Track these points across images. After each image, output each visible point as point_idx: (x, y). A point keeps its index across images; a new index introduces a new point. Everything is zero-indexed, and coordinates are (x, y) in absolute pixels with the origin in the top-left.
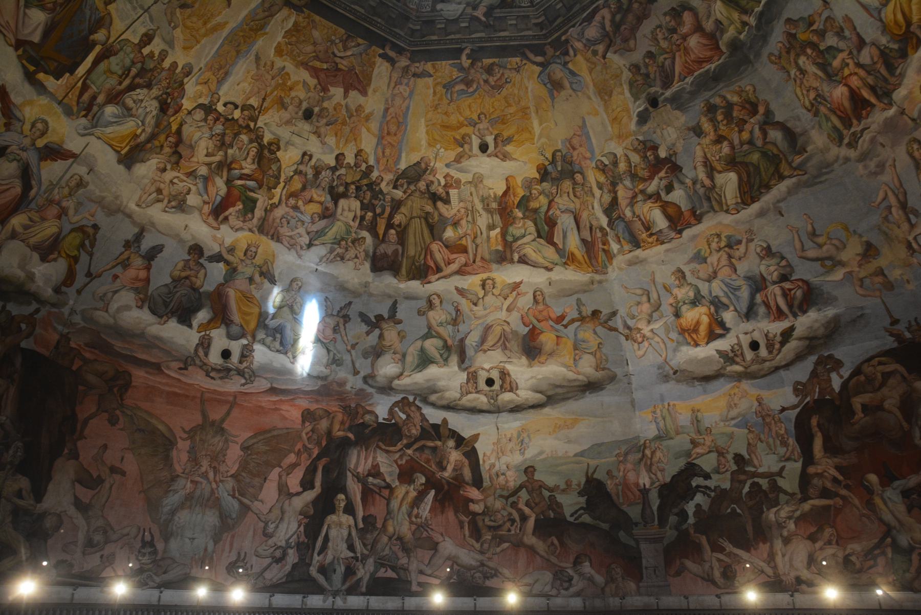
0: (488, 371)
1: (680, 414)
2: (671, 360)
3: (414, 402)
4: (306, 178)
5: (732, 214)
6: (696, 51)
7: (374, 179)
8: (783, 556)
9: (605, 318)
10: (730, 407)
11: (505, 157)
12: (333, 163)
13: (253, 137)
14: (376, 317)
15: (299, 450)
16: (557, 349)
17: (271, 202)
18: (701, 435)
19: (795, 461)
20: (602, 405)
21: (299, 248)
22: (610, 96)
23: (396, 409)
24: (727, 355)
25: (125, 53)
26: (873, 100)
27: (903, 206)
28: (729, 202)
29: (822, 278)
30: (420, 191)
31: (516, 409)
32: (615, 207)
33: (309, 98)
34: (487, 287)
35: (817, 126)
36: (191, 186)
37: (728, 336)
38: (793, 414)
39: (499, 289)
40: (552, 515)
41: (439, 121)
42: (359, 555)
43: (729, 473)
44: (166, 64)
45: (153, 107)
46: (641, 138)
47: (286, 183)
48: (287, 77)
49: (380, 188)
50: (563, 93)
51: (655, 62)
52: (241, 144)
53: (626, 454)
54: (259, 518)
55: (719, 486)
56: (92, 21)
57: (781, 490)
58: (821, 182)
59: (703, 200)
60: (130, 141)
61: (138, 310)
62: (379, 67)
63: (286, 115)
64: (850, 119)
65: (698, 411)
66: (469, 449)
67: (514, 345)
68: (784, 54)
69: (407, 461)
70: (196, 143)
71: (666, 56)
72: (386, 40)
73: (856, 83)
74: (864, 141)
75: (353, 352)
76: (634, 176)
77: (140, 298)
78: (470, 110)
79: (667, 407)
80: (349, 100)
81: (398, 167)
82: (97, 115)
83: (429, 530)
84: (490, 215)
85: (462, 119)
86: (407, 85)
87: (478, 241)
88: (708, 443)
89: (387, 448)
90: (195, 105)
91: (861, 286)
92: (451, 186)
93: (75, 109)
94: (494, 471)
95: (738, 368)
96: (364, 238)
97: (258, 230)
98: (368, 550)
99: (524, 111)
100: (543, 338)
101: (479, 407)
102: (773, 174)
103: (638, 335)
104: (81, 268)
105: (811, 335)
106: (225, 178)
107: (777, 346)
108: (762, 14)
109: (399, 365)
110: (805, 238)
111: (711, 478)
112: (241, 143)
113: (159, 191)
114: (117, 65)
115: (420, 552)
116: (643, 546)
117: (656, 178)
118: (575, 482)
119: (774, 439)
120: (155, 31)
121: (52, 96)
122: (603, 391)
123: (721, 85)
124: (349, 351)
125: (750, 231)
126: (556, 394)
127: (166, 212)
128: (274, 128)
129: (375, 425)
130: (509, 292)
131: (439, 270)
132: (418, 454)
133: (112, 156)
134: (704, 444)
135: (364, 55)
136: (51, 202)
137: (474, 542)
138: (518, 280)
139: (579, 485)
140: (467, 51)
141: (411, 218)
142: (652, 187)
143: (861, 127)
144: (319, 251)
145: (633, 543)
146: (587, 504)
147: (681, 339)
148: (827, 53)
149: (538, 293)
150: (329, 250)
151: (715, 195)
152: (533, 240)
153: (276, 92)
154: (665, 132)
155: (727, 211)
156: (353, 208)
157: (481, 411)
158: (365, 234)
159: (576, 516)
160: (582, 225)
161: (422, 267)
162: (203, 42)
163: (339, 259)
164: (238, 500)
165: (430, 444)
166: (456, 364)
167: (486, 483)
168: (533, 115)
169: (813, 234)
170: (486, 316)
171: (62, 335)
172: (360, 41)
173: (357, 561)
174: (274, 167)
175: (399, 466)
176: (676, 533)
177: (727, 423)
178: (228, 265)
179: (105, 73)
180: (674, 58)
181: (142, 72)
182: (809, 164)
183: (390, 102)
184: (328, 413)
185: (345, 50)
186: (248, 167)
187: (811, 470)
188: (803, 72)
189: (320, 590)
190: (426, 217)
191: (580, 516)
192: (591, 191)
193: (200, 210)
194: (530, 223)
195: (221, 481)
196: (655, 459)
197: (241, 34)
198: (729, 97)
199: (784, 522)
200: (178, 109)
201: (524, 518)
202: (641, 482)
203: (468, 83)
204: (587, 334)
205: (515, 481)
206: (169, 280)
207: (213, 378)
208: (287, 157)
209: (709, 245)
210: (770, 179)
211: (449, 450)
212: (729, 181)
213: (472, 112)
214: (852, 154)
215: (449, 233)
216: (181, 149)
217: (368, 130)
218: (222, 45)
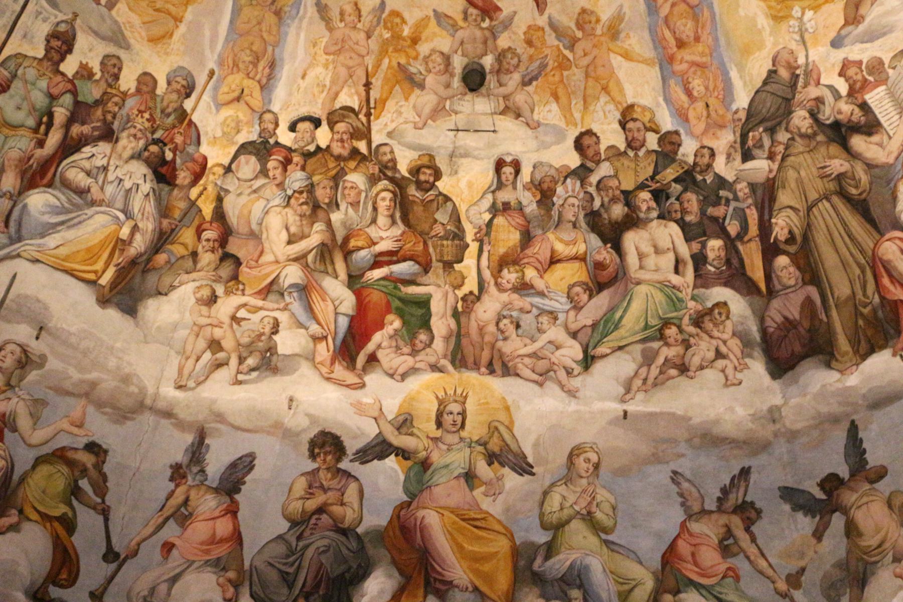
4: (523, 215)
7: (691, 160)
12: (574, 160)
14: (822, 485)
17: (460, 293)
21: (562, 374)
25: (26, 82)
30: (802, 136)
33: (462, 43)
36: (277, 314)
44: (128, 81)
48: (398, 20)
49: (716, 173)
52: (353, 193)
63: (426, 99)
77: (230, 581)
81: (734, 107)
90: (234, 149)
92: (865, 85)
97: (453, 362)
112: (353, 193)
113: (215, 345)
114: (19, 108)
120: (71, 23)
127: (240, 383)
128: (412, 136)
133: (84, 296)
141: (809, 209)
150: (639, 358)
156: (665, 243)
158: (720, 293)
162: (189, 15)
163: (673, 372)
174: (442, 216)
178: (406, 459)
193: (311, 358)
200: (200, 170)
206: (283, 526)
208: (463, 184)
216: (232, 248)
218: (237, 11)
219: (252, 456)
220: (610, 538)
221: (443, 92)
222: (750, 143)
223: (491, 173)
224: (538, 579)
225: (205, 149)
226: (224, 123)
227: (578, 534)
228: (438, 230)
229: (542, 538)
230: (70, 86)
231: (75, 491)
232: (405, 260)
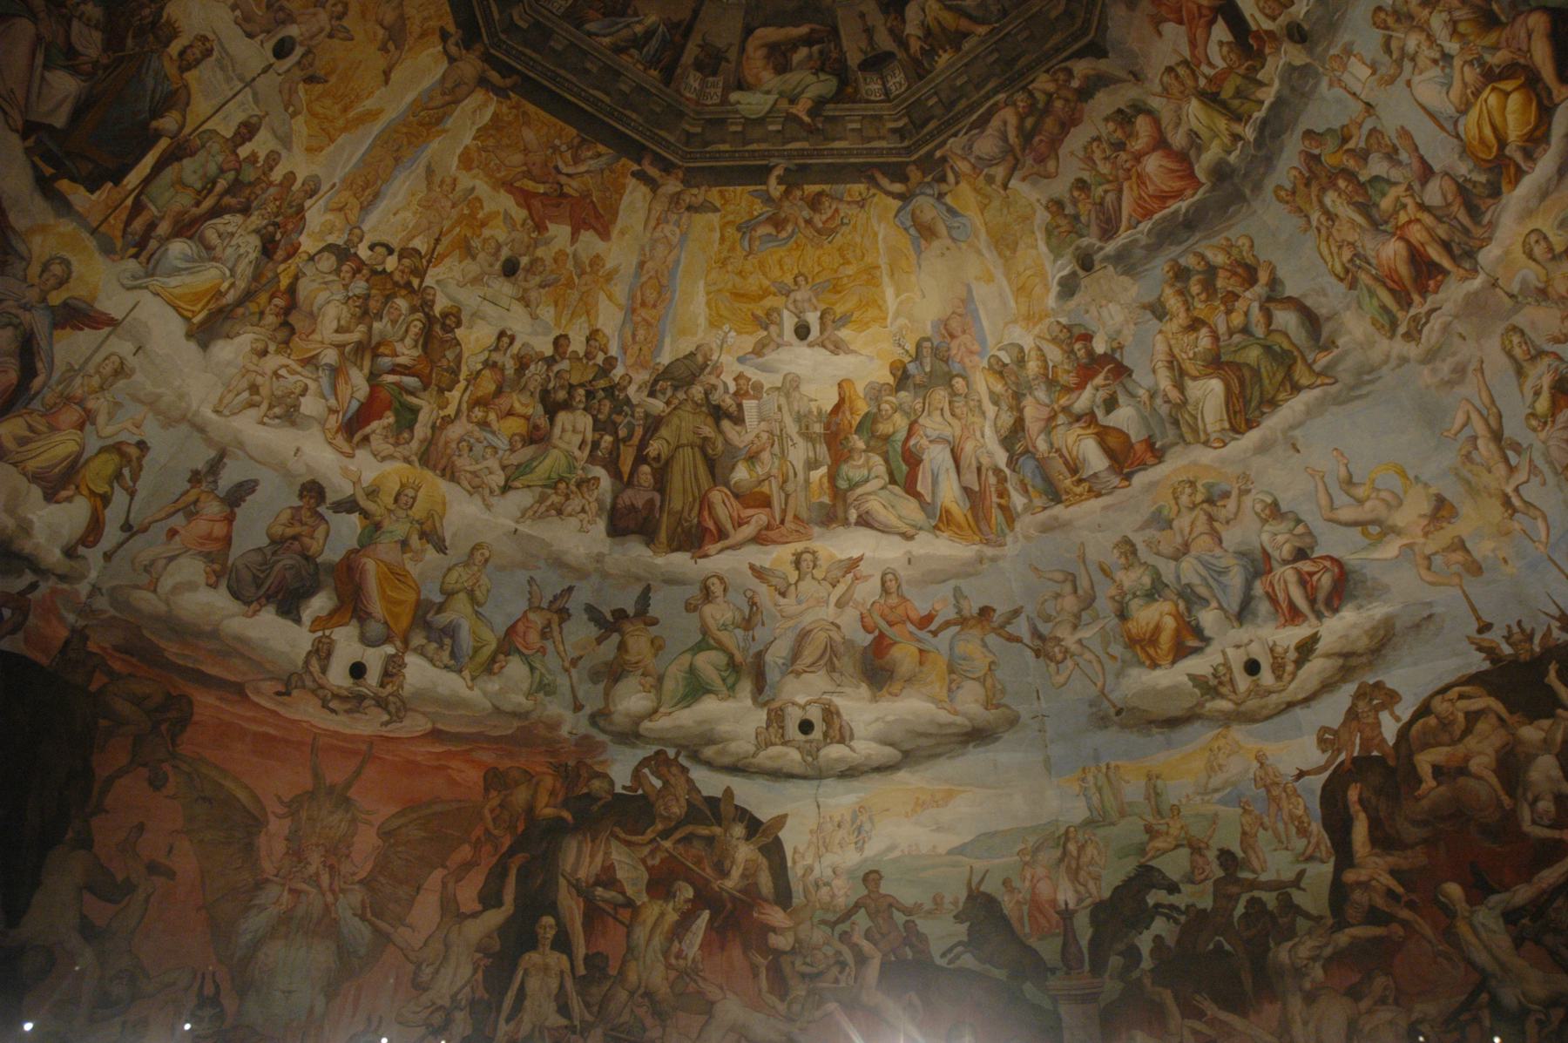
0: (803, 708)
1: (1128, 782)
2: (1112, 691)
5: (1215, 448)
6: (1158, 182)
7: (617, 380)
10: (1212, 769)
11: (838, 347)
12: (549, 351)
13: (417, 302)
14: (614, 612)
15: (479, 838)
16: (921, 672)
17: (442, 413)
19: (1323, 862)
21: (487, 492)
22: (1014, 251)
23: (646, 771)
24: (1207, 683)
25: (209, 153)
26: (1446, 263)
27: (1497, 436)
28: (1210, 428)
29: (1363, 555)
31: (850, 773)
32: (1020, 434)
33: (513, 240)
34: (804, 565)
36: (309, 382)
37: (1209, 650)
41: (730, 285)
42: (577, 1023)
43: (1210, 883)
44: (277, 175)
45: (250, 245)
46: (1064, 320)
47: (469, 382)
49: (627, 396)
50: (936, 244)
51: (1088, 197)
52: (396, 313)
53: (1037, 850)
54: (406, 956)
55: (1193, 905)
56: (157, 97)
57: (1298, 911)
59: (1167, 425)
60: (209, 302)
61: (212, 592)
62: (631, 193)
63: (472, 268)
64: (1408, 294)
67: (846, 663)
68: (1301, 187)
69: (662, 861)
70: (320, 309)
71: (1106, 187)
72: (644, 148)
73: (1418, 236)
74: (1432, 329)
75: (573, 671)
76: (1051, 383)
77: (214, 571)
78: (781, 268)
79: (1104, 770)
80: (577, 245)
81: (658, 360)
82: (156, 256)
84: (810, 445)
85: (766, 283)
86: (677, 224)
87: (790, 487)
88: (1174, 831)
89: (629, 838)
90: (322, 245)
91: (1429, 568)
93: (119, 244)
94: (811, 878)
95: (1224, 705)
96: (597, 479)
97: (420, 460)
98: (591, 1013)
99: (871, 275)
100: (896, 653)
102: (1282, 383)
104: (113, 516)
105: (1345, 651)
106: (366, 371)
107: (1290, 668)
108: (1264, 122)
109: (652, 695)
110: (1335, 490)
111: (1179, 891)
112: (396, 313)
113: (254, 388)
114: (195, 172)
117: (1089, 387)
118: (948, 899)
119: (1286, 824)
120: (261, 118)
121: (81, 219)
123: (1198, 235)
124: (567, 670)
125: (1245, 477)
127: (264, 424)
129: (610, 798)
130: (840, 574)
131: (722, 534)
133: (177, 326)
134: (1167, 833)
135: (607, 173)
136: (68, 400)
138: (855, 555)
139: (955, 903)
140: (778, 172)
141: (678, 447)
142: (1083, 401)
143: (1427, 307)
144: (521, 498)
146: (969, 935)
147: (1128, 655)
148: (1372, 187)
149: (890, 576)
150: (537, 497)
151: (1186, 416)
152: (882, 488)
153: (458, 229)
154: (1104, 312)
155: (1206, 443)
156: (580, 427)
157: (790, 776)
158: (599, 472)
160: (963, 464)
161: (694, 530)
162: (340, 140)
163: (553, 512)
164: (372, 924)
166: (749, 695)
167: (798, 899)
168: (886, 279)
169: (1349, 482)
170: (801, 613)
171: (73, 630)
172: (601, 148)
173: (574, 1033)
174: (450, 355)
175: (648, 869)
176: (1119, 986)
177: (1206, 798)
178: (366, 518)
179: (173, 185)
180: (1120, 191)
181: (236, 187)
182: (1341, 367)
183: (647, 249)
184: (528, 775)
185: (575, 163)
186: (407, 353)
187: (1350, 876)
188: (1331, 217)
190: (703, 445)
191: (958, 957)
192: (980, 406)
193: (322, 423)
194: (877, 460)
195: (342, 891)
196: (1084, 860)
197: (405, 130)
198: (1209, 255)
199: (1306, 966)
200: (293, 251)
202: (1061, 898)
203: (778, 223)
204: (971, 646)
206: (265, 541)
207: (333, 711)
208: (473, 338)
209: (1176, 498)
211: (734, 842)
212: (1210, 393)
213: (784, 273)
214: (1412, 350)
215: (741, 474)
216: (292, 319)
217: (610, 297)
218: (372, 147)
219: (256, 482)
220: (480, 610)
222: (658, 387)
223: (494, 338)
224: (427, 626)
225: (303, 239)
226: (323, 224)
227: (461, 603)
228: (444, 363)
229: (438, 598)
230: (237, 165)
231: (118, 476)
232: (413, 375)
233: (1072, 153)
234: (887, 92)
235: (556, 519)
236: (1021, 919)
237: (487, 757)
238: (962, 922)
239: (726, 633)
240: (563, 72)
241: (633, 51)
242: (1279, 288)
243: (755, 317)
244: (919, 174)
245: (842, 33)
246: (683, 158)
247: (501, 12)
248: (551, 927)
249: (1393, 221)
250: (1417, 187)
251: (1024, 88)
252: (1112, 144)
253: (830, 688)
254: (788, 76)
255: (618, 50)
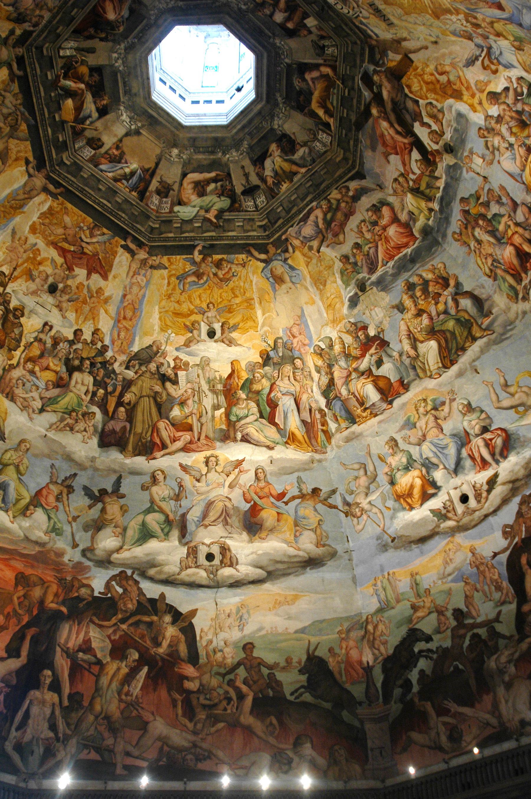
1: (400, 581)
2: (389, 528)
3: (132, 576)
7: (108, 358)
8: (507, 702)
9: (326, 495)
10: (446, 563)
11: (231, 343)
12: (71, 337)
15: (9, 613)
17: (9, 362)
18: (420, 598)
19: (510, 603)
20: (323, 581)
21: (31, 410)
22: (325, 285)
23: (114, 583)
24: (440, 513)
28: (432, 368)
29: (517, 424)
30: (150, 372)
31: (236, 584)
34: (210, 464)
35: (498, 289)
37: (440, 494)
38: (504, 558)
39: (222, 465)
40: (271, 693)
41: (172, 309)
43: (449, 630)
46: (352, 320)
47: (25, 347)
50: (284, 286)
53: (349, 631)
55: (441, 646)
58: (507, 339)
59: (410, 370)
63: (33, 286)
64: (520, 275)
65: (417, 574)
66: (187, 624)
67: (234, 520)
68: (464, 230)
69: (121, 637)
75: (74, 524)
76: (347, 356)
79: (386, 576)
80: (90, 281)
83: (139, 709)
85: (192, 307)
86: (145, 275)
87: (203, 420)
89: (101, 623)
92: (180, 368)
94: (211, 647)
95: (451, 523)
98: (70, 730)
99: (249, 303)
100: (264, 514)
101: (198, 581)
102: (467, 337)
103: (357, 510)
105: (513, 478)
107: (484, 494)
108: (442, 198)
109: (120, 539)
110: (499, 391)
115: (128, 733)
116: (368, 726)
117: (367, 355)
118: (295, 660)
119: (489, 585)
122: (324, 568)
123: (418, 265)
124: (70, 523)
125: (453, 392)
126: (277, 570)
128: (21, 296)
129: (90, 599)
131: (164, 446)
132: (132, 629)
135: (108, 244)
137: (187, 721)
138: (240, 458)
139: (299, 662)
140: (199, 248)
141: (141, 397)
142: (364, 364)
144: (50, 418)
145: (357, 724)
147: (397, 505)
149: (260, 470)
151: (419, 363)
152: (256, 420)
154: (373, 313)
155: (431, 377)
156: (86, 382)
157: (200, 586)
158: (95, 409)
159: (296, 694)
160: (302, 407)
163: (68, 429)
165: (147, 619)
167: (203, 660)
168: (257, 305)
169: (506, 385)
170: (208, 492)
172: (105, 230)
174: (17, 331)
175: (112, 641)
176: (400, 706)
180: (377, 247)
182: (496, 324)
184: (43, 582)
187: (526, 608)
188: (479, 242)
189: (14, 770)
190: (155, 396)
191: (301, 695)
192: (310, 375)
194: (253, 405)
196: (378, 633)
198: (424, 275)
199: (505, 667)
201: (241, 697)
202: (364, 660)
203: (199, 275)
205: (232, 657)
208: (30, 324)
209: (417, 410)
210: (465, 342)
211: (165, 625)
215: (176, 412)
217: (106, 312)
221: (40, 288)
223: (41, 325)
233: (351, 230)
234: (256, 206)
235: (69, 433)
236: (340, 673)
237: (19, 565)
238: (304, 674)
239: (164, 503)
240: (87, 189)
241: (124, 181)
242: (460, 288)
243: (186, 326)
244: (274, 249)
245: (233, 176)
246: (149, 241)
247: (57, 155)
248: (49, 676)
249: (506, 236)
250: (512, 214)
251: (326, 198)
252: (371, 223)
253: (225, 534)
254: (205, 198)
255: (116, 180)
